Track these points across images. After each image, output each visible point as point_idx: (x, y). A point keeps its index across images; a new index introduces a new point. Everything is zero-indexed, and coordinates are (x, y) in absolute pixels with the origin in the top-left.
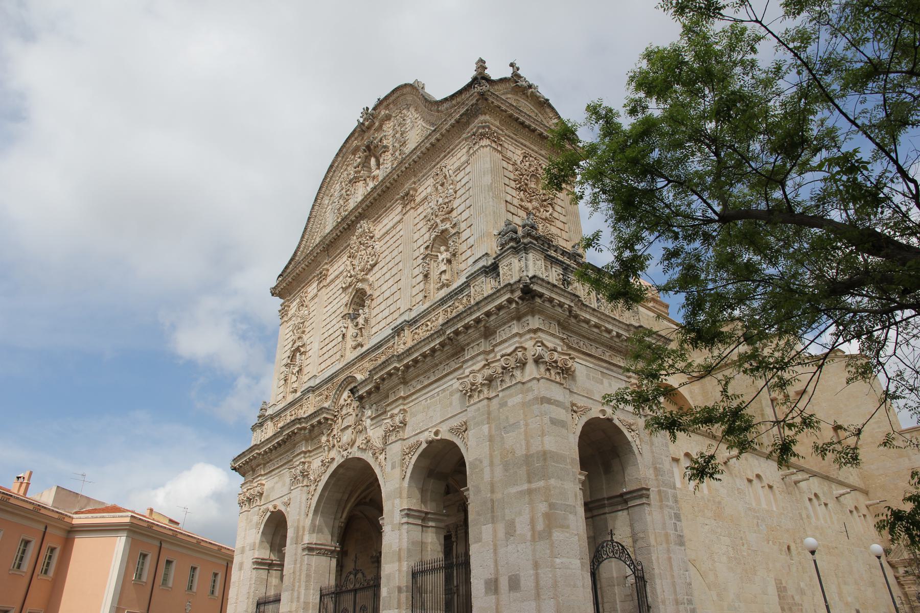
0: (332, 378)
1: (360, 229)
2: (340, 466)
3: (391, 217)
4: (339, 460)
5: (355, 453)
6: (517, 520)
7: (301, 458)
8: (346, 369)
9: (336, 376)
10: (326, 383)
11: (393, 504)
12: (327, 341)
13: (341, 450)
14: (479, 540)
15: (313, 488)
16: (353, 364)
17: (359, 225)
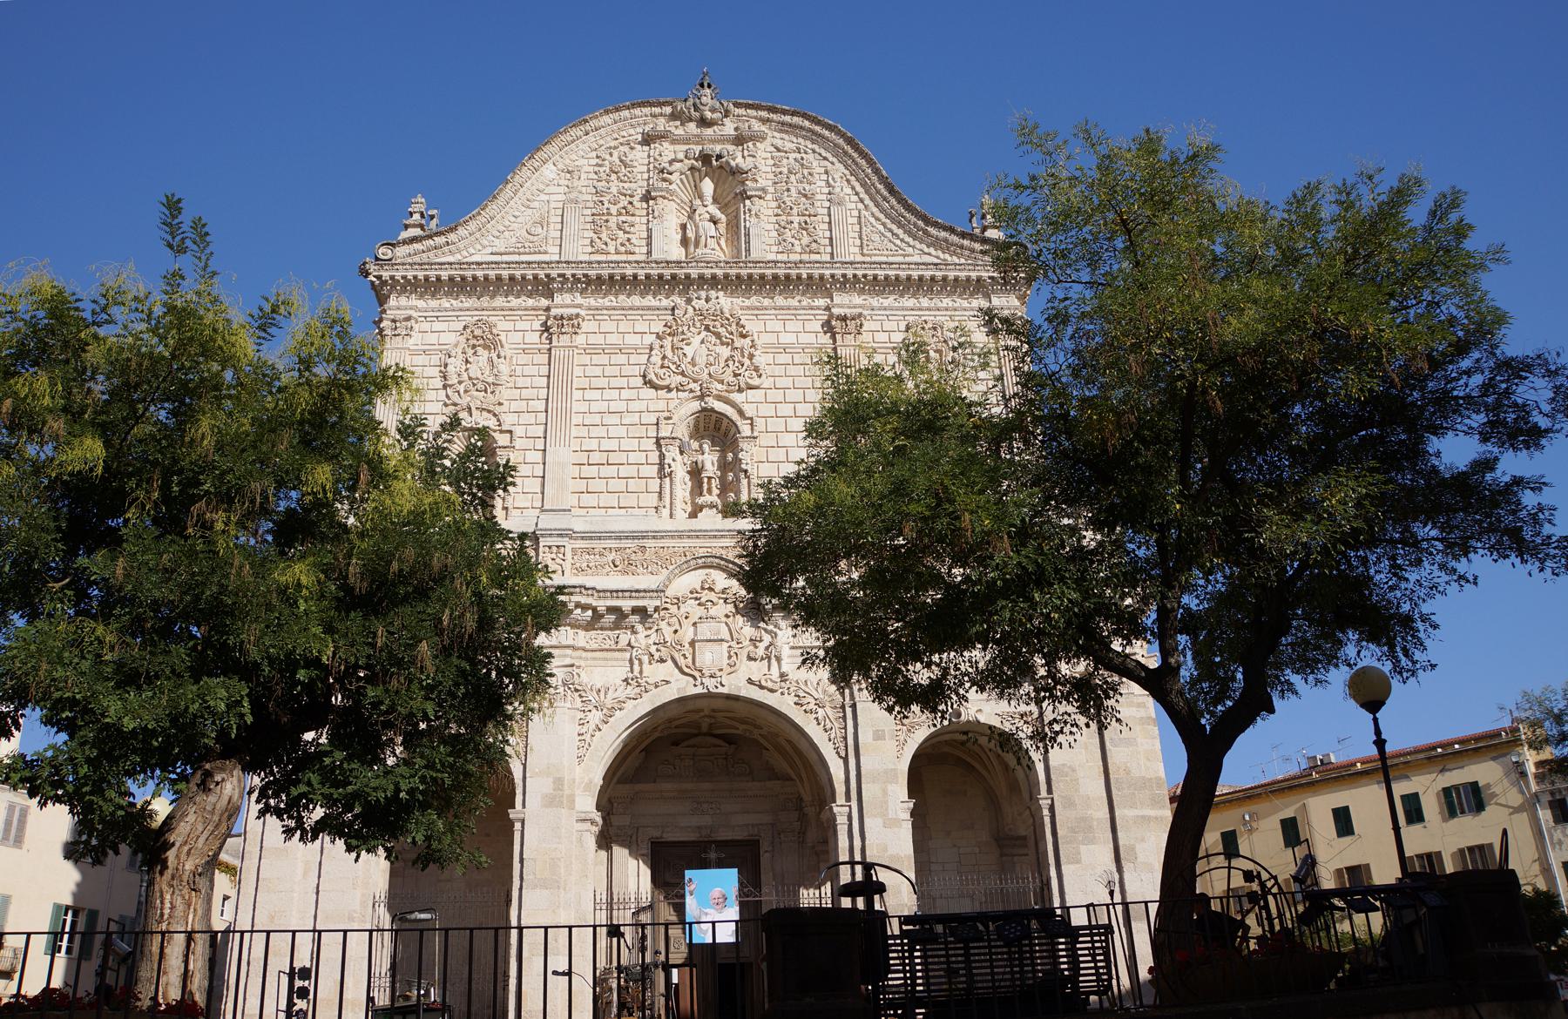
0: (643, 537)
1: (703, 302)
2: (681, 701)
3: (791, 326)
4: (681, 687)
5: (736, 684)
6: (1138, 846)
7: (565, 656)
8: (689, 537)
9: (654, 537)
10: (619, 538)
11: (885, 793)
12: (595, 457)
13: (697, 674)
14: (1078, 862)
15: (595, 717)
16: (715, 537)
17: (703, 294)
